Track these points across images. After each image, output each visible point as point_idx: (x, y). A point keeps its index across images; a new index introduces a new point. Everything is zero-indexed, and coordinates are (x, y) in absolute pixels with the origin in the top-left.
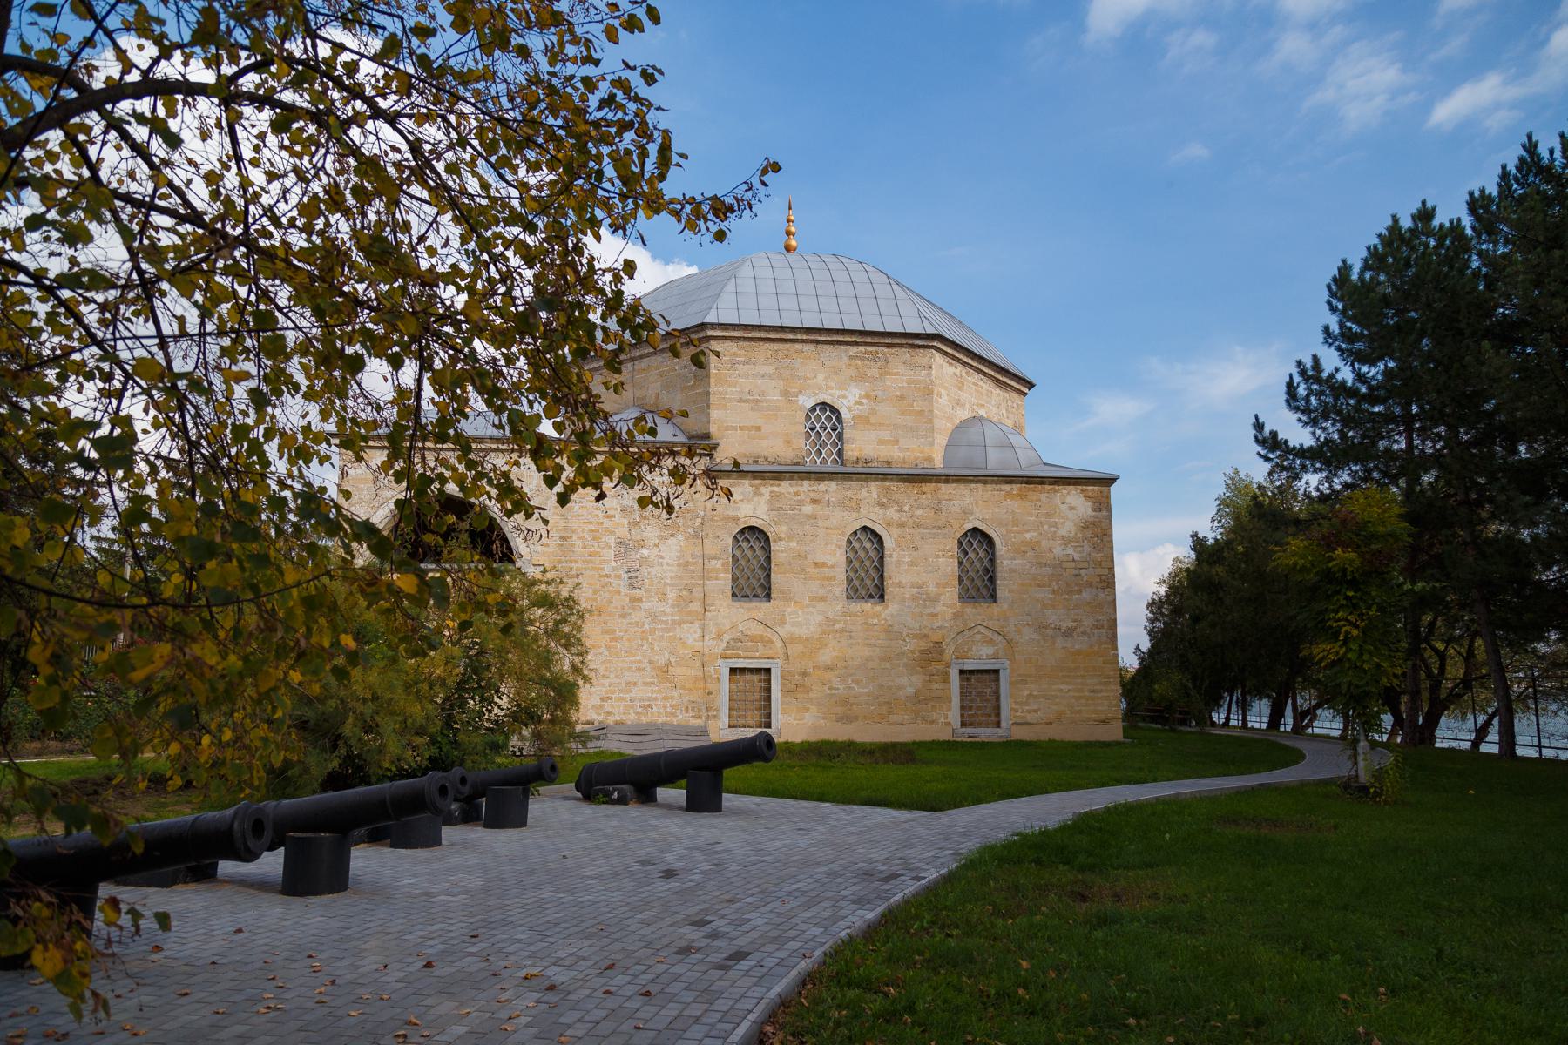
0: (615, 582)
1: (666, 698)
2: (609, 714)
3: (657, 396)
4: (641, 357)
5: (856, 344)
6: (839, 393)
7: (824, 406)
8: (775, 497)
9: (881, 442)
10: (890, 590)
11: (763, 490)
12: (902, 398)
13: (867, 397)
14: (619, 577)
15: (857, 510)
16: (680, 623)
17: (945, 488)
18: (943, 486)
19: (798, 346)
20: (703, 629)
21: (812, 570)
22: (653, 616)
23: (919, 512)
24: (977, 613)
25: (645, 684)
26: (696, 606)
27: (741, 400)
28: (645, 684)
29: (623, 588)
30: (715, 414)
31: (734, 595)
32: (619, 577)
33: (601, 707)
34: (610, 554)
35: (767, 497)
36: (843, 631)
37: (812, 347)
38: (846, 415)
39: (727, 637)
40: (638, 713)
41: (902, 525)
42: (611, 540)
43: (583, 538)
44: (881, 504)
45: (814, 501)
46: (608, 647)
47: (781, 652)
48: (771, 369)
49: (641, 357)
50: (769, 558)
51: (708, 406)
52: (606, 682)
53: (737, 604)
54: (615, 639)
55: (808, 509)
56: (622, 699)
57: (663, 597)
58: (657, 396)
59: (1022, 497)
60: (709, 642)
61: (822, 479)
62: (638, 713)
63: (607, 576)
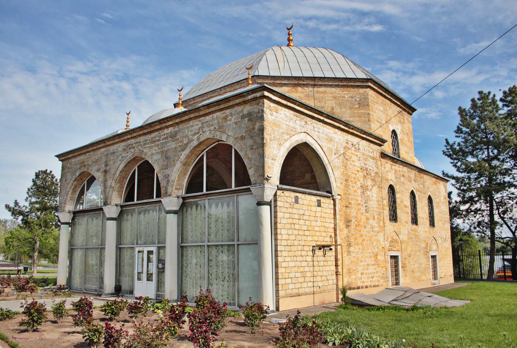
0: (362, 208)
1: (377, 272)
2: (363, 282)
3: (333, 109)
4: (321, 85)
5: (398, 106)
6: (397, 127)
7: (394, 132)
8: (396, 171)
9: (406, 152)
10: (419, 220)
11: (393, 167)
12: (407, 134)
13: (402, 131)
14: (362, 205)
15: (410, 182)
16: (378, 232)
17: (426, 177)
18: (425, 176)
19: (387, 101)
20: (384, 235)
21: (404, 208)
22: (372, 227)
23: (421, 186)
24: (432, 230)
25: (372, 265)
26: (382, 223)
27: (378, 122)
28: (372, 265)
29: (364, 212)
30: (372, 125)
31: (390, 219)
32: (362, 205)
33: (361, 278)
34: (359, 191)
35: (393, 172)
36: (411, 238)
37: (389, 102)
38: (399, 138)
39: (389, 240)
40: (371, 281)
41: (419, 191)
42: (359, 184)
43: (351, 181)
44: (415, 180)
45: (403, 176)
46: (362, 245)
47: (400, 247)
48: (382, 108)
49: (321, 85)
50: (394, 202)
51: (369, 120)
52: (362, 264)
53: (391, 223)
54: (363, 240)
55: (402, 179)
56: (366, 274)
57: (374, 219)
58: (333, 109)
59: (435, 184)
60: (386, 243)
61: (404, 166)
62: (371, 281)
63: (359, 204)
